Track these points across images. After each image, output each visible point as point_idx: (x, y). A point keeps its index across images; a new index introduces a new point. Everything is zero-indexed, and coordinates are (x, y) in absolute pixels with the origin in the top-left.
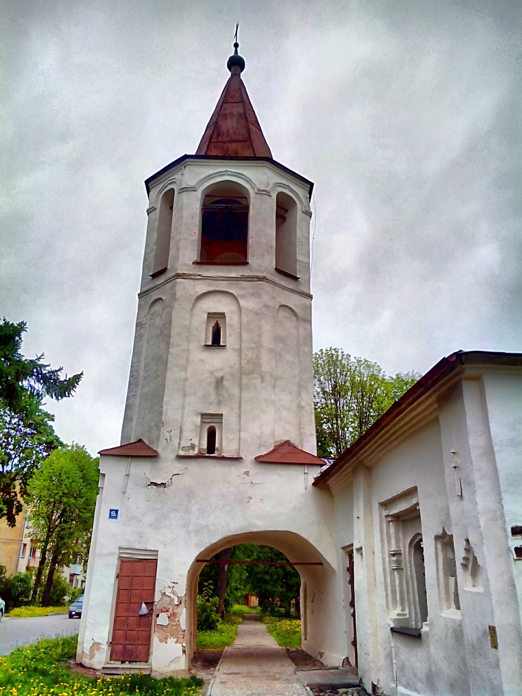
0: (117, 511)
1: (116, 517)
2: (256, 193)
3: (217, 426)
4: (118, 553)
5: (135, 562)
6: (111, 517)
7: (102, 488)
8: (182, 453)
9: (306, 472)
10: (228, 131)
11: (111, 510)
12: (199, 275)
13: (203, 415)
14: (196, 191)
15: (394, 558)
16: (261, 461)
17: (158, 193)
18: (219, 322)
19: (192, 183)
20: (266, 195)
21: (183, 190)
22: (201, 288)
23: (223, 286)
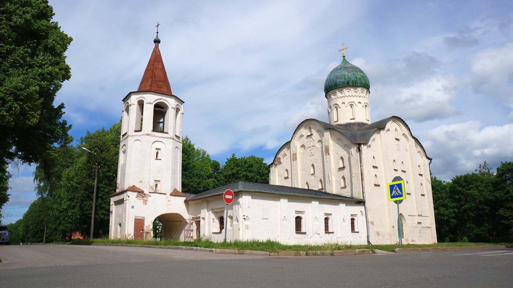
1: (133, 208)
6: (132, 208)
8: (150, 191)
10: (158, 76)
12: (154, 135)
19: (152, 102)
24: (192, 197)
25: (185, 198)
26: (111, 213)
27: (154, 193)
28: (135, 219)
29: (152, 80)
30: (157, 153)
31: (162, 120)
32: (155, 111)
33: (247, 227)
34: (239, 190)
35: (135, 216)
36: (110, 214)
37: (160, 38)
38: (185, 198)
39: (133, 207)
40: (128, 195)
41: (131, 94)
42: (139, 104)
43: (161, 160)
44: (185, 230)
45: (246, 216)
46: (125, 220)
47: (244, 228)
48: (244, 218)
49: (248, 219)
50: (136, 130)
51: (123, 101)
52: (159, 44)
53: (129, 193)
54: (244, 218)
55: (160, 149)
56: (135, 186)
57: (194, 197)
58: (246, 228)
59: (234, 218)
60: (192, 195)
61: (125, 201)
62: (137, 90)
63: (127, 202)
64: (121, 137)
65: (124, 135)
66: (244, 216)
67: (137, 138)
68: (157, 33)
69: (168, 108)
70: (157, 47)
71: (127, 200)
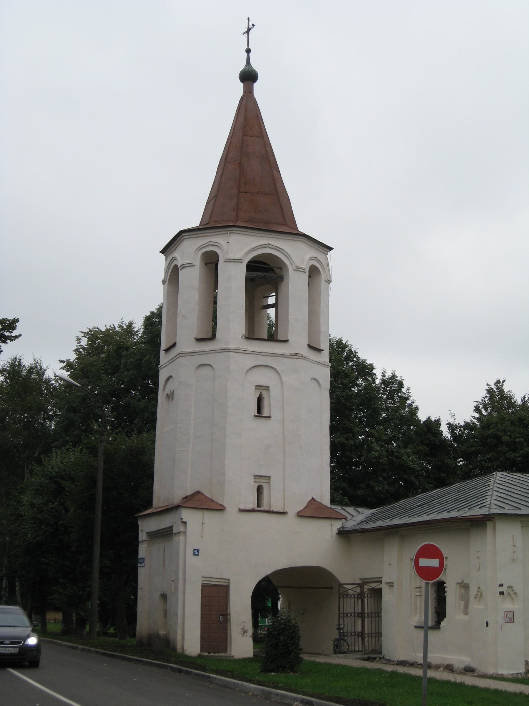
0: (198, 550)
1: (198, 555)
2: (294, 270)
3: (265, 486)
4: (201, 580)
5: (210, 586)
6: (194, 554)
7: (185, 533)
9: (332, 524)
11: (194, 550)
13: (255, 476)
14: (242, 262)
15: (418, 590)
16: (301, 515)
17: (196, 250)
18: (263, 393)
20: (302, 272)
21: (229, 261)
22: (251, 361)
23: (268, 361)
24: (360, 518)
25: (337, 525)
26: (141, 563)
27: (253, 511)
28: (204, 586)
29: (239, 192)
30: (260, 400)
31: (271, 300)
32: (249, 281)
33: (509, 617)
34: (484, 511)
35: (203, 577)
36: (139, 565)
37: (255, 66)
38: (337, 525)
39: (196, 552)
40: (184, 520)
41: (183, 234)
42: (206, 264)
43: (269, 417)
44: (342, 615)
45: (505, 586)
46: (176, 589)
47: (501, 620)
48: (502, 593)
49: (511, 593)
50: (199, 338)
51: (163, 252)
52: (255, 85)
53: (186, 514)
54: (502, 593)
55: (267, 388)
56: (203, 494)
57: (367, 520)
58: (507, 620)
59: (473, 591)
60: (360, 510)
61: (175, 533)
62: (196, 223)
63: (181, 538)
64: (162, 353)
65: (167, 350)
66: (501, 585)
67: (205, 359)
68: (248, 51)
69: (287, 269)
70: (248, 93)
71: (180, 532)
